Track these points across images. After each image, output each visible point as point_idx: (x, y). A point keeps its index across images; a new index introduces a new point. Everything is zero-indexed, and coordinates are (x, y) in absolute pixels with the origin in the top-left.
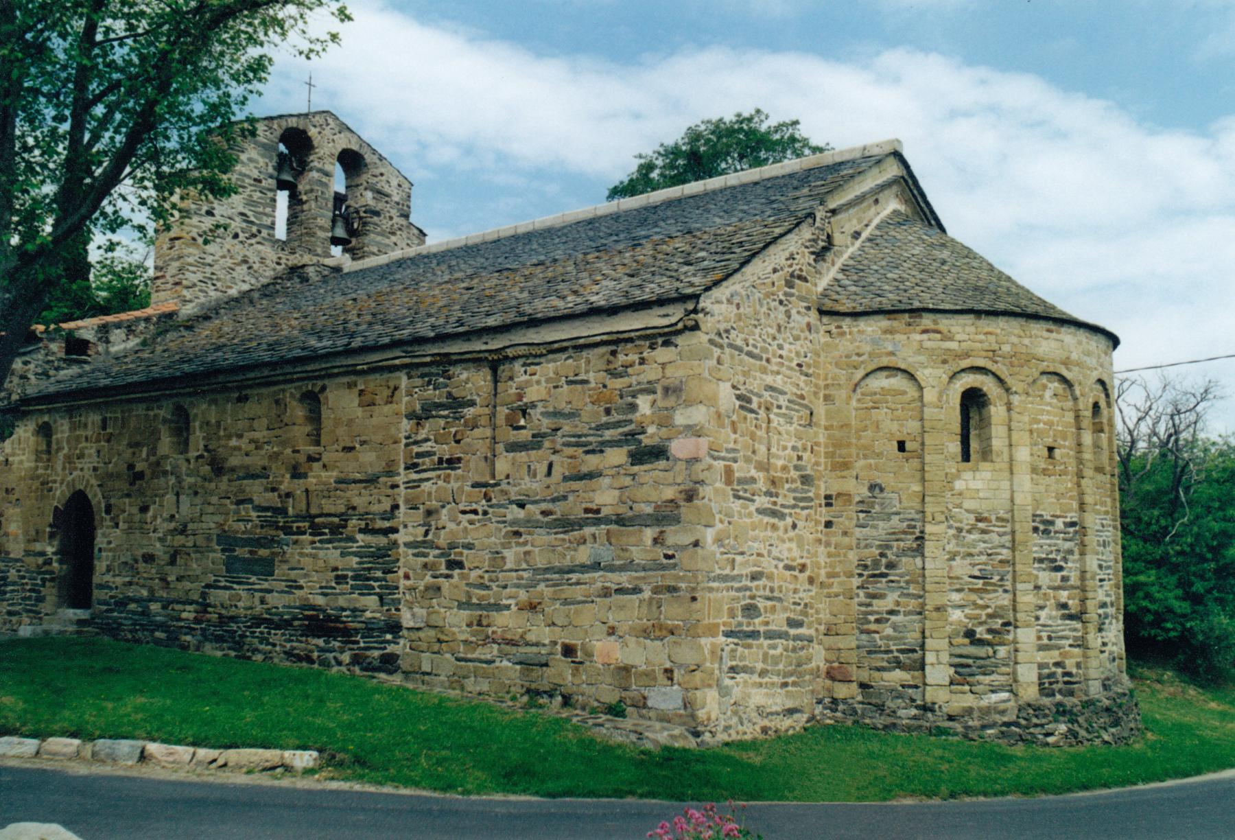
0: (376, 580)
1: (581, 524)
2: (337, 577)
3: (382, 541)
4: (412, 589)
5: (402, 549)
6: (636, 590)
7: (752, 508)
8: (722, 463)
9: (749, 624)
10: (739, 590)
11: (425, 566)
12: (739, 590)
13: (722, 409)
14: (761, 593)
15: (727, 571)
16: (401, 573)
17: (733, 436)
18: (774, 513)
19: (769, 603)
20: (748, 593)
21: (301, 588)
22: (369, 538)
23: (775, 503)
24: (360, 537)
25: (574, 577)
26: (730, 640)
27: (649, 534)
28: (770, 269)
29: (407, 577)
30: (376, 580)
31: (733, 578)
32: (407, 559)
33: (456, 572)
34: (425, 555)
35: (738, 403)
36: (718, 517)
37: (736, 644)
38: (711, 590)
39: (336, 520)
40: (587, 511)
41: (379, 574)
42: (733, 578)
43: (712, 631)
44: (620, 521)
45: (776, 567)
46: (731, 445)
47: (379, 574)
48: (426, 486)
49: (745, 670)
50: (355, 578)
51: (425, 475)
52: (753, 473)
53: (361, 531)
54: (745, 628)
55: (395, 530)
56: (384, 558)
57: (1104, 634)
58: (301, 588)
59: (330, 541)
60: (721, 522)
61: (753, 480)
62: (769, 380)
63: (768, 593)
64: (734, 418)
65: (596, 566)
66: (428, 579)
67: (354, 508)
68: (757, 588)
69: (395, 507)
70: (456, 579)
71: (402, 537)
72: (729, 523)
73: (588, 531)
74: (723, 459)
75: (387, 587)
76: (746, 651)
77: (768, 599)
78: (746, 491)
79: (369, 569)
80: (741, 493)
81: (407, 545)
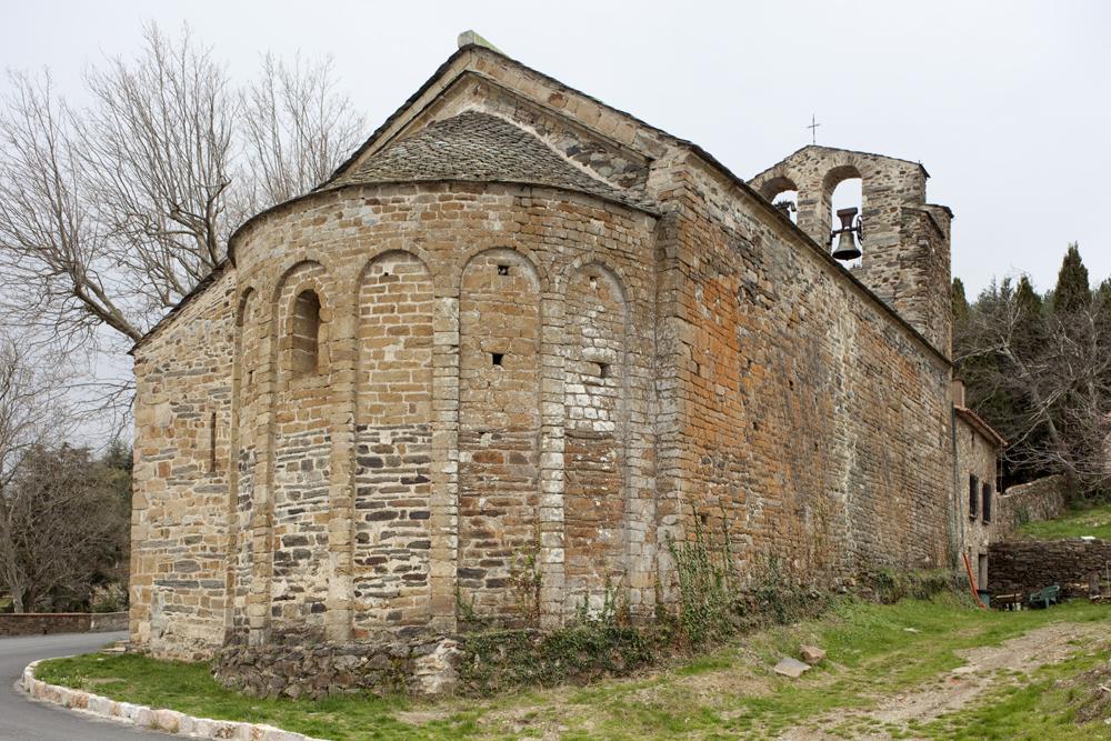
7: (190, 489)
8: (157, 462)
9: (184, 576)
10: (174, 551)
12: (174, 551)
13: (158, 424)
14: (201, 552)
15: (162, 539)
17: (169, 440)
18: (216, 490)
19: (208, 561)
20: (183, 553)
23: (219, 481)
26: (163, 588)
28: (223, 293)
31: (167, 543)
35: (176, 414)
36: (150, 502)
37: (171, 591)
38: (144, 552)
42: (167, 543)
43: (147, 580)
45: (219, 531)
46: (169, 446)
49: (178, 609)
52: (193, 462)
54: (179, 579)
57: (293, 577)
60: (154, 504)
61: (193, 467)
62: (216, 384)
63: (208, 552)
64: (172, 426)
68: (194, 549)
72: (163, 504)
74: (158, 459)
76: (181, 596)
77: (209, 557)
78: (182, 477)
80: (177, 480)
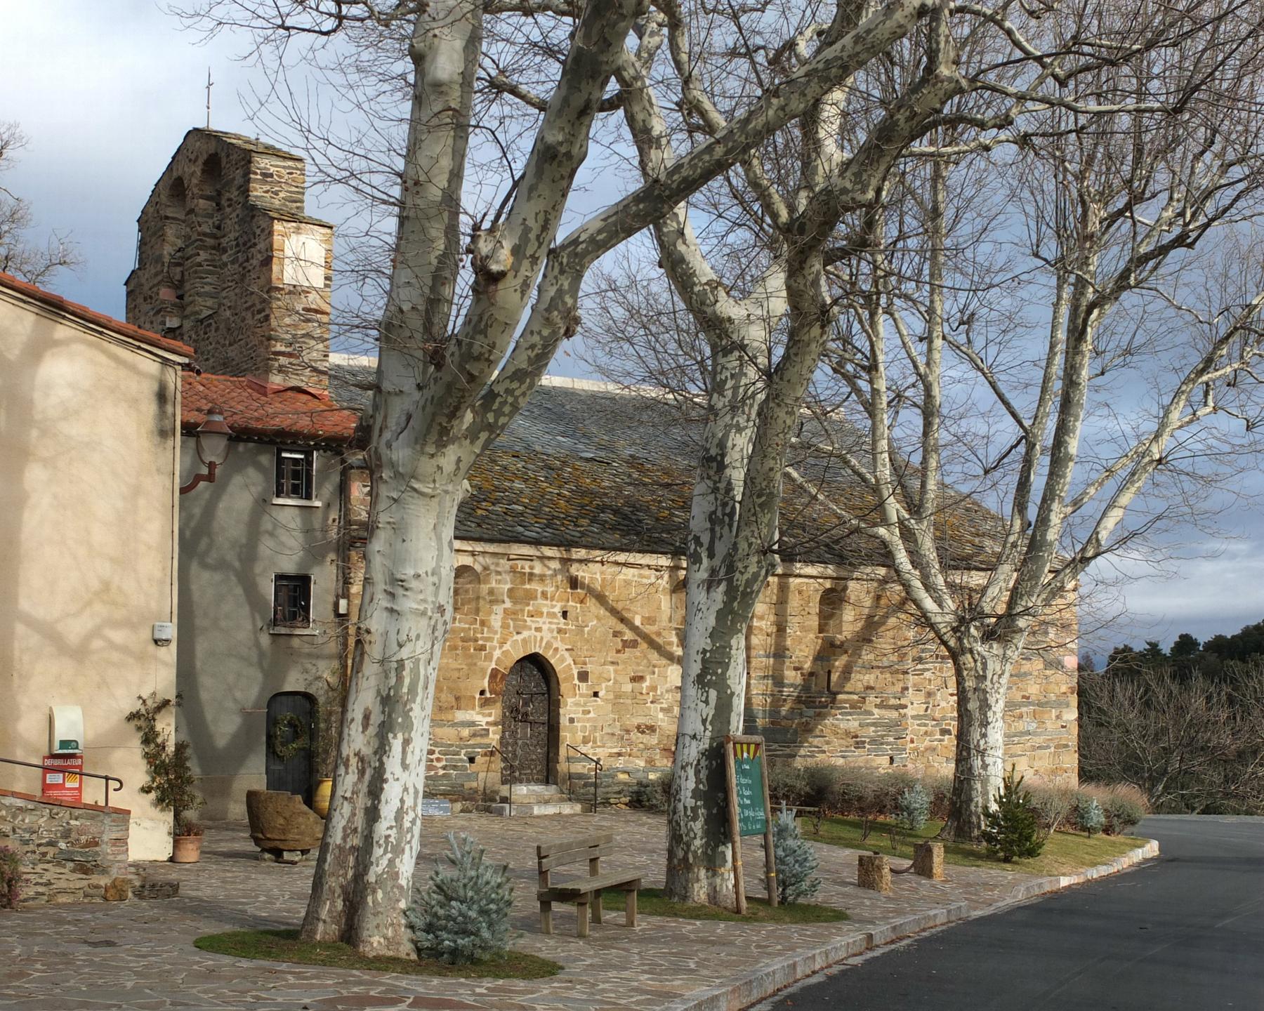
0: (888, 744)
1: (1020, 705)
2: (857, 743)
3: (894, 714)
4: (916, 749)
5: (910, 721)
6: (1048, 747)
11: (926, 733)
16: (908, 738)
21: (824, 752)
22: (883, 712)
24: (876, 711)
25: (1016, 739)
27: (1054, 713)
29: (912, 741)
30: (888, 744)
32: (912, 725)
33: (947, 737)
34: (925, 725)
39: (855, 697)
40: (1024, 697)
41: (891, 739)
44: (1040, 704)
47: (891, 739)
48: (927, 675)
50: (869, 743)
51: (927, 666)
53: (876, 706)
55: (905, 707)
56: (896, 727)
58: (824, 752)
59: (850, 714)
65: (1028, 733)
66: (927, 743)
67: (872, 688)
69: (907, 689)
70: (946, 742)
71: (909, 712)
73: (1024, 709)
75: (898, 749)
79: (883, 736)
81: (913, 717)
